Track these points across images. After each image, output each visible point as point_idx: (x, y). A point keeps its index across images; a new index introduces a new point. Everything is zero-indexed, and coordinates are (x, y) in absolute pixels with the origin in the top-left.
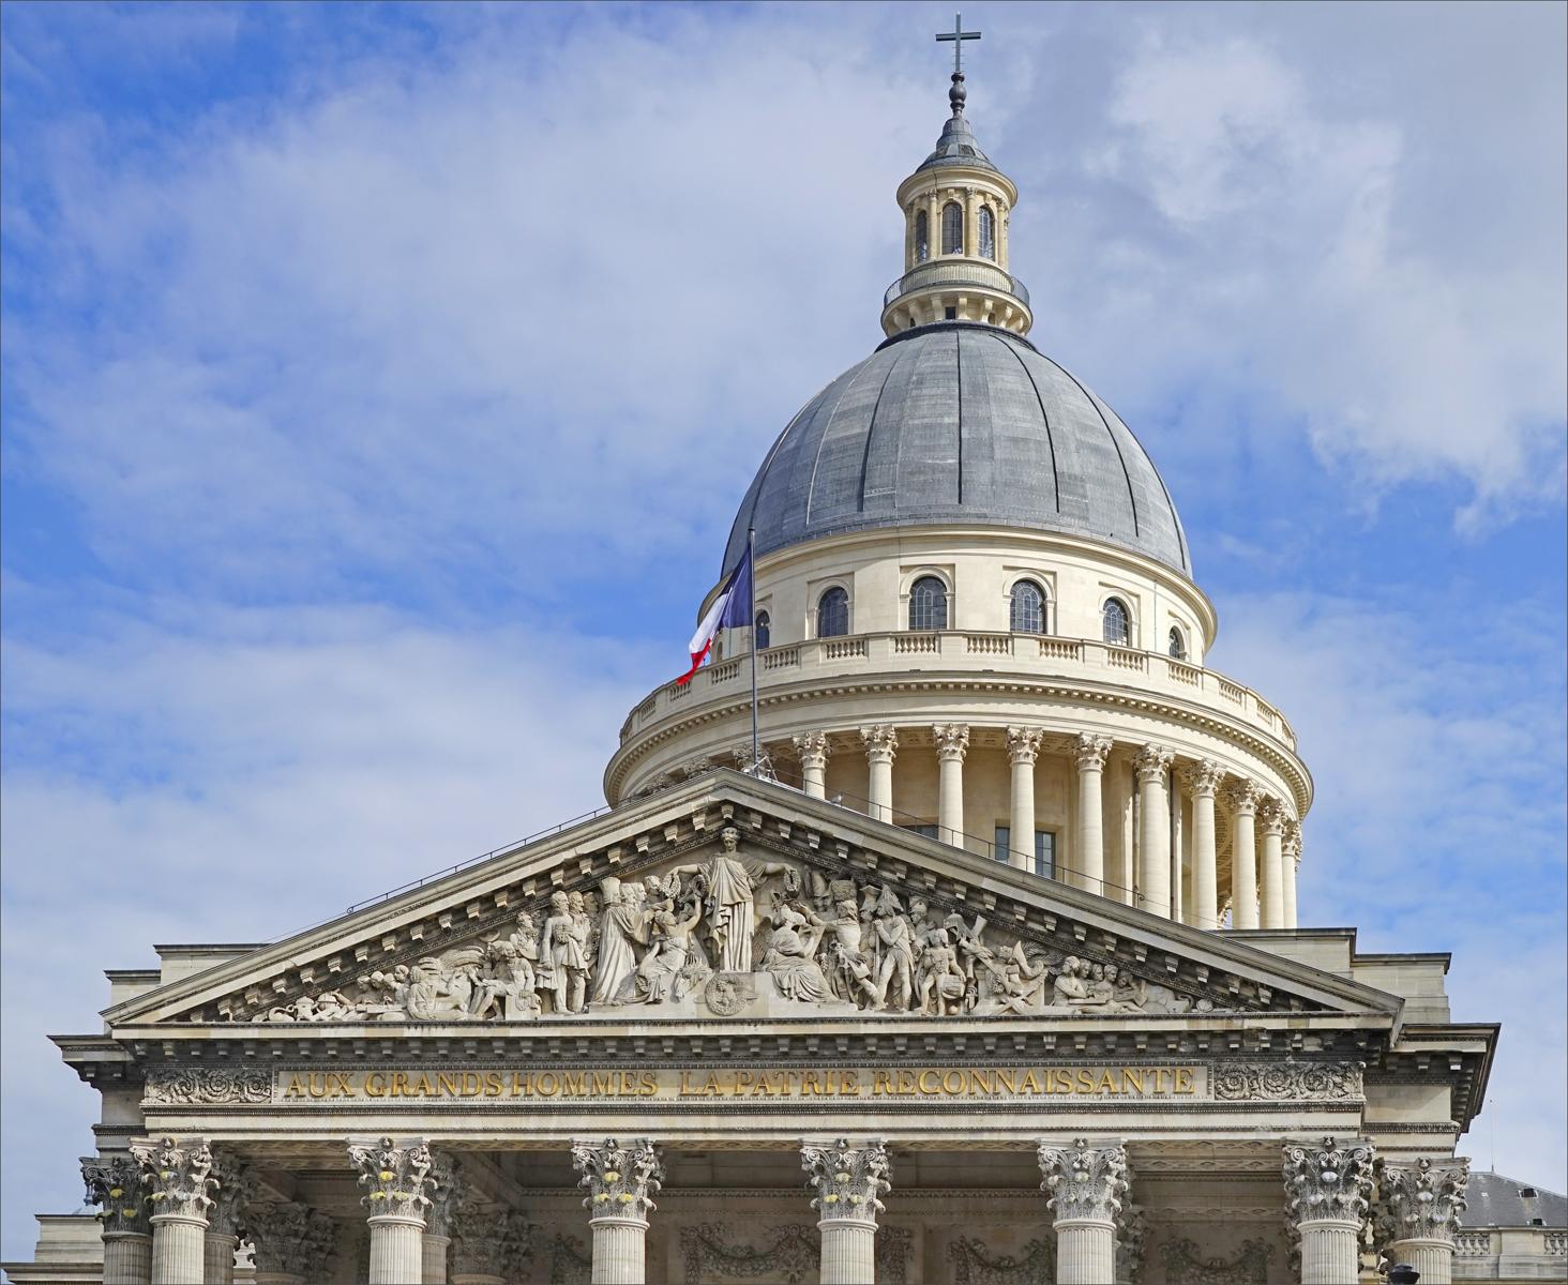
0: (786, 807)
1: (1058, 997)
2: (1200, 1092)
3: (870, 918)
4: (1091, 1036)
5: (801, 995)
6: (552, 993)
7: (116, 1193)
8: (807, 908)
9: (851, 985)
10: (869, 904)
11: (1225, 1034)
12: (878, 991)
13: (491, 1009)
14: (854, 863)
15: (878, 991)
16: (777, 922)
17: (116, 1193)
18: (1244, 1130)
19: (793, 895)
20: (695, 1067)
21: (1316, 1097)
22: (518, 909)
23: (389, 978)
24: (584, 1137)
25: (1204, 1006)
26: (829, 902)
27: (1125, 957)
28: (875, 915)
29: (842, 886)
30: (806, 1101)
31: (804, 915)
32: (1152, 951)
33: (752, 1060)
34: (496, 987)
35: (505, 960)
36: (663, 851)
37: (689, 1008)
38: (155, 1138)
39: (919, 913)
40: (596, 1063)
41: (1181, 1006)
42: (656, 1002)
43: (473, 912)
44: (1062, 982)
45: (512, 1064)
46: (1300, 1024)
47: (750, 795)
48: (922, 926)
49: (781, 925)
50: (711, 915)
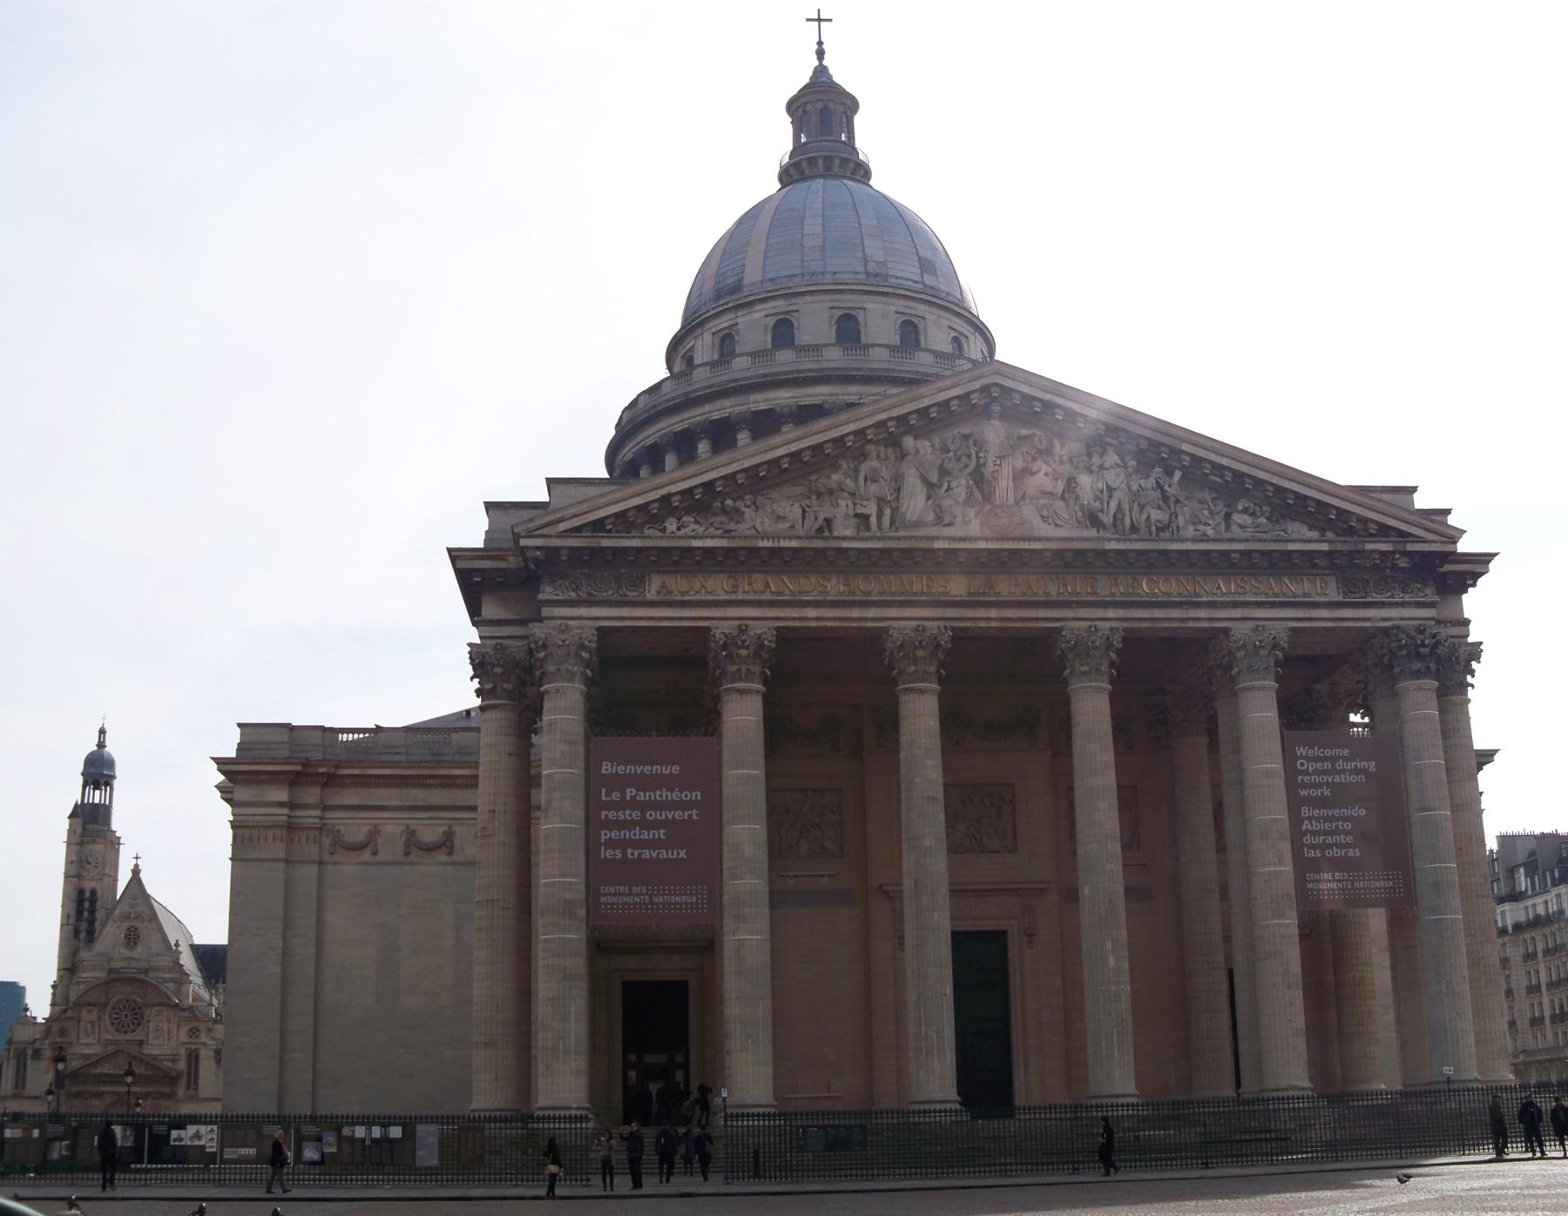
1: (1235, 528)
2: (1334, 594)
4: (1263, 553)
6: (866, 518)
7: (498, 670)
10: (1096, 460)
11: (1351, 552)
12: (1107, 519)
13: (820, 530)
15: (1107, 519)
17: (498, 670)
18: (1364, 619)
19: (1040, 452)
21: (1407, 598)
22: (837, 456)
23: (739, 504)
24: (901, 621)
25: (1330, 535)
27: (1276, 501)
28: (1101, 467)
32: (1298, 496)
34: (825, 511)
35: (831, 492)
38: (552, 623)
41: (1315, 534)
42: (950, 524)
43: (806, 457)
44: (1237, 518)
46: (1400, 547)
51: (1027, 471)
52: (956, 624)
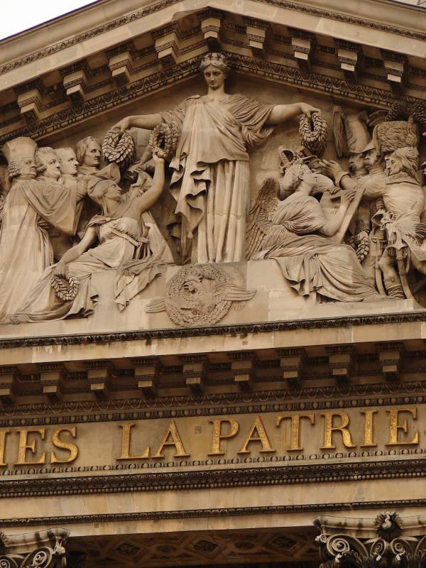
0: (304, 10)
5: (321, 292)
8: (337, 169)
9: (408, 276)
14: (415, 94)
16: (285, 183)
20: (142, 417)
26: (372, 159)
29: (389, 130)
30: (327, 460)
31: (333, 179)
36: (108, 97)
37: (137, 320)
42: (83, 314)
49: (292, 190)
50: (178, 184)
51: (270, 191)
52: (75, 532)
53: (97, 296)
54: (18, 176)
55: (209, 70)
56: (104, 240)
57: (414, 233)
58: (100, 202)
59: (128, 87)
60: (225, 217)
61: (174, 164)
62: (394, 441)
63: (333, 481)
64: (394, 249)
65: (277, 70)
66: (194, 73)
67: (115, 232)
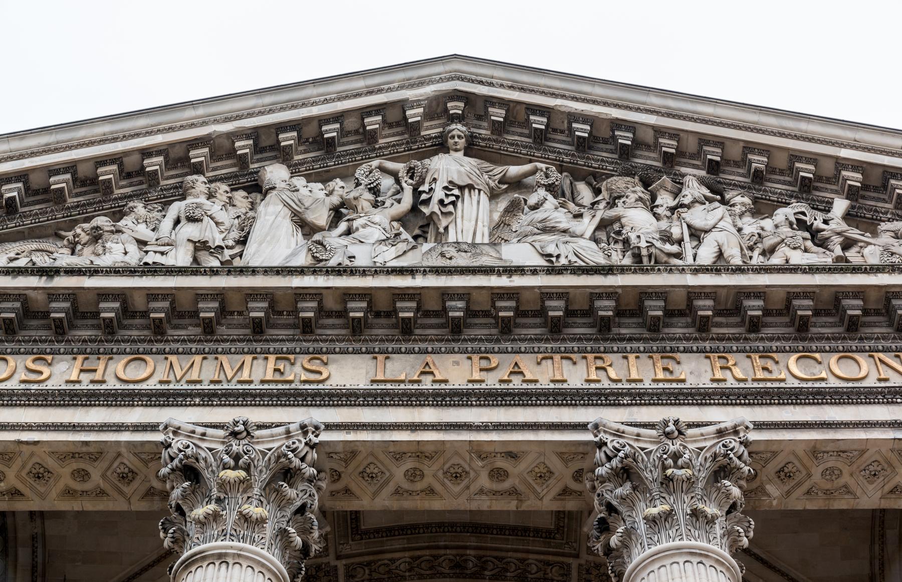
3: (669, 214)
10: (665, 200)
22: (130, 197)
29: (619, 183)
33: (498, 341)
39: (743, 204)
40: (227, 345)
45: (76, 347)
47: (491, 84)
48: (747, 219)
50: (427, 202)
53: (354, 257)
54: (274, 188)
55: (454, 133)
56: (357, 229)
57: (657, 236)
58: (354, 203)
59: (377, 146)
60: (473, 222)
61: (425, 187)
62: (661, 375)
63: (602, 405)
64: (639, 248)
65: (512, 145)
66: (435, 145)
67: (369, 223)
